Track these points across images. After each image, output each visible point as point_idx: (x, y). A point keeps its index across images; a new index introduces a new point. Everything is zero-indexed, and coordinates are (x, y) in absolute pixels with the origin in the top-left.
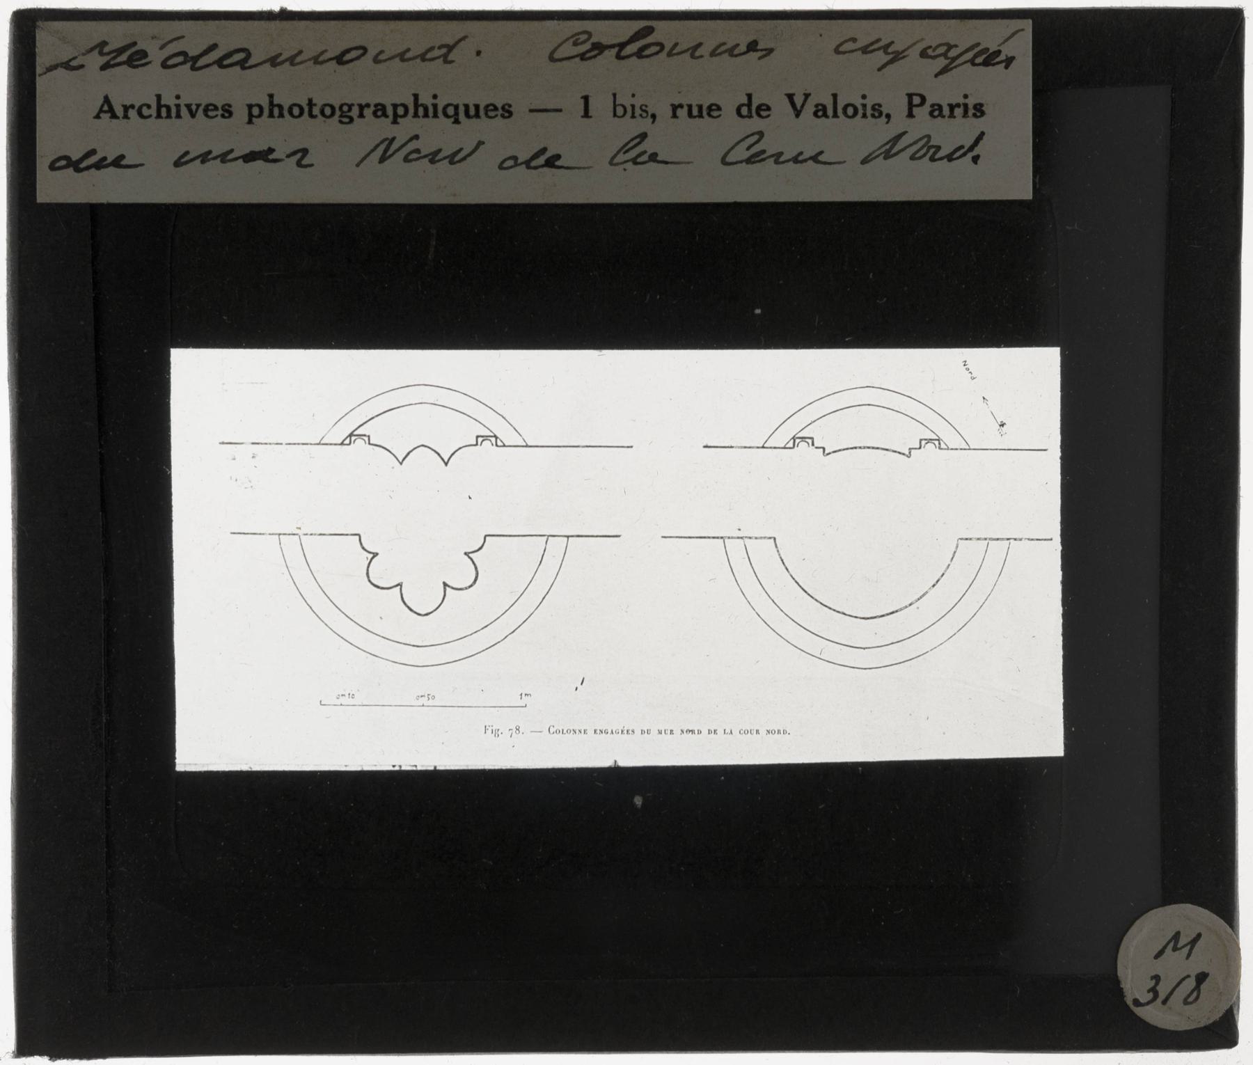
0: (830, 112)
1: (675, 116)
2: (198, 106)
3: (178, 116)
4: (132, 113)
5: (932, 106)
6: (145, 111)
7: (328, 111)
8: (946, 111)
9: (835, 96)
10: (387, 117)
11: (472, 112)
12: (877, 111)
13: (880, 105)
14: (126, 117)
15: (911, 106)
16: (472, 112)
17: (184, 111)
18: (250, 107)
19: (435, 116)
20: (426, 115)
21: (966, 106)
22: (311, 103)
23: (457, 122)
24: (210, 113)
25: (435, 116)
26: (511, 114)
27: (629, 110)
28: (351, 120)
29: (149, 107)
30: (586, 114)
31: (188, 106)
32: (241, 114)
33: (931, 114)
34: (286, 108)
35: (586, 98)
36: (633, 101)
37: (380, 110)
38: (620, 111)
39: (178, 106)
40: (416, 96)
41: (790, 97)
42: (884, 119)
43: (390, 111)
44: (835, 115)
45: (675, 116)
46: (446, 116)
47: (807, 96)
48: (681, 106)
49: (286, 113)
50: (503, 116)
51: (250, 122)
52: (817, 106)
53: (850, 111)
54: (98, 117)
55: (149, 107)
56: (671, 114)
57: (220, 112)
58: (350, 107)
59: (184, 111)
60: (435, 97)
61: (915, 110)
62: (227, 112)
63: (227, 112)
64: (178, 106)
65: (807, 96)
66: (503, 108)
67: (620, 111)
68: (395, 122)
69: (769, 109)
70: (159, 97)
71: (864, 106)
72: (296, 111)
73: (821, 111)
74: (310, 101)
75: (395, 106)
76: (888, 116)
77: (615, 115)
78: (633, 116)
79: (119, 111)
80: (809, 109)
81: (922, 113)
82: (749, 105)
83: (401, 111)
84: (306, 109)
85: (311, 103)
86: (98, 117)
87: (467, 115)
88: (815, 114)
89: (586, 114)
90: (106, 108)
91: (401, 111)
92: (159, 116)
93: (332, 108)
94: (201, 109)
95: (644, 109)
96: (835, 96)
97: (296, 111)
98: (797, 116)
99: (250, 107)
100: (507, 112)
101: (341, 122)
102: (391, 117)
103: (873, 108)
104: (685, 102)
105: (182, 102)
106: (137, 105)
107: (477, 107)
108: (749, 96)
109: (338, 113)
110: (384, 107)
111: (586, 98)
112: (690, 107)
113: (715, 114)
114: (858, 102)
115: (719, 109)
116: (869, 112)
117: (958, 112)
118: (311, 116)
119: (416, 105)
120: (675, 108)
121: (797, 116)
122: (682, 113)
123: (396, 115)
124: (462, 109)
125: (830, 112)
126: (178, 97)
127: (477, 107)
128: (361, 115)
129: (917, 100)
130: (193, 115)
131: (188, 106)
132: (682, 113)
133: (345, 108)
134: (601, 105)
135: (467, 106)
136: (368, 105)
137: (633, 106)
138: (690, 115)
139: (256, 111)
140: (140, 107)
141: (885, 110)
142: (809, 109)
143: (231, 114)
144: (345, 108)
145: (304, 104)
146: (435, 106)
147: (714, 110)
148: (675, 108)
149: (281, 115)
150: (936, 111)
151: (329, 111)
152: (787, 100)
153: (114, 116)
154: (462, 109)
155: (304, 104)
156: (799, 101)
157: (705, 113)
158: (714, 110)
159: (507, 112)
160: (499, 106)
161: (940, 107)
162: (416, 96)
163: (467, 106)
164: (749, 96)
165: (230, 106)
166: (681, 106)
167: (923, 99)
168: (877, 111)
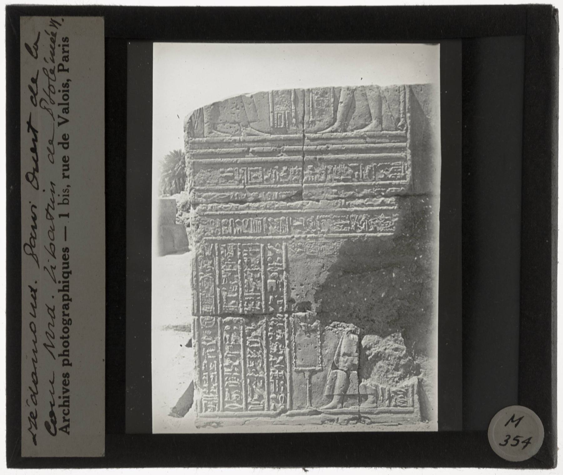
0: (66, 106)
1: (68, 177)
2: (63, 388)
3: (68, 397)
4: (67, 418)
5: (63, 60)
6: (66, 412)
7: (66, 330)
8: (66, 54)
9: (59, 104)
10: (68, 304)
11: (66, 266)
12: (66, 85)
13: (63, 84)
14: (68, 420)
15: (64, 70)
16: (66, 266)
17: (66, 395)
18: (64, 365)
19: (68, 282)
20: (68, 286)
21: (63, 46)
22: (63, 338)
23: (70, 272)
24: (67, 382)
25: (68, 282)
26: (67, 248)
27: (64, 197)
28: (70, 319)
29: (64, 410)
30: (68, 215)
31: (64, 393)
32: (67, 369)
33: (67, 61)
34: (65, 349)
35: (60, 216)
36: (61, 196)
37: (66, 307)
38: (66, 201)
39: (64, 397)
40: (59, 291)
41: (59, 124)
42: (69, 82)
43: (66, 302)
44: (68, 104)
45: (68, 177)
46: (67, 277)
47: (59, 117)
48: (63, 174)
49: (67, 349)
50: (68, 252)
51: (71, 365)
52: (63, 112)
53: (66, 97)
54: (68, 433)
55: (64, 410)
56: (67, 179)
57: (66, 378)
58: (64, 320)
59: (66, 395)
60: (59, 282)
61: (66, 68)
62: (66, 375)
63: (66, 375)
64: (64, 397)
65: (59, 117)
66: (64, 252)
67: (66, 201)
68: (71, 300)
69: (65, 135)
70: (60, 406)
71: (63, 91)
72: (66, 344)
73: (66, 111)
74: (61, 338)
75: (64, 300)
76: (68, 80)
77: (68, 204)
78: (68, 196)
79: (66, 423)
80: (65, 116)
81: (66, 65)
82: (63, 144)
83: (66, 297)
84: (65, 340)
85: (63, 338)
86: (68, 433)
87: (68, 268)
88: (67, 113)
89: (68, 215)
90: (65, 429)
91: (66, 297)
92: (68, 406)
93: (64, 328)
94: (65, 387)
95: (65, 191)
96: (59, 104)
97: (66, 344)
98: (67, 121)
99: (64, 365)
100: (66, 250)
101: (71, 324)
102: (69, 302)
103: (64, 87)
104: (62, 172)
105: (62, 396)
106: (64, 415)
107: (64, 263)
108: (59, 143)
109: (67, 325)
110: (65, 305)
111: (60, 216)
112: (64, 170)
113: (67, 159)
114: (62, 94)
115: (65, 157)
116: (66, 89)
117: (66, 49)
118: (68, 337)
119: (63, 290)
120: (64, 177)
121: (67, 121)
122: (67, 173)
123: (68, 300)
124: (65, 270)
125: (66, 106)
126: (60, 397)
127: (64, 263)
128: (68, 315)
129: (61, 68)
130: (68, 391)
131: (64, 393)
132: (67, 173)
133: (65, 322)
134: (63, 209)
135: (64, 268)
136: (63, 312)
137: (63, 196)
138: (68, 170)
139: (66, 362)
140: (64, 413)
141: (65, 82)
142: (65, 116)
143: (68, 374)
144: (65, 322)
145: (62, 341)
146: (64, 282)
147: (65, 160)
148: (64, 177)
149: (68, 351)
150: (66, 59)
151: (66, 330)
152: (60, 126)
153: (68, 426)
154: (65, 270)
155: (62, 341)
156: (61, 120)
157: (67, 163)
158: (65, 160)
159: (66, 250)
160: (63, 253)
161: (64, 57)
162: (59, 291)
163: (64, 268)
164: (59, 143)
165: (64, 374)
166: (63, 174)
167: (61, 64)
168: (66, 85)
